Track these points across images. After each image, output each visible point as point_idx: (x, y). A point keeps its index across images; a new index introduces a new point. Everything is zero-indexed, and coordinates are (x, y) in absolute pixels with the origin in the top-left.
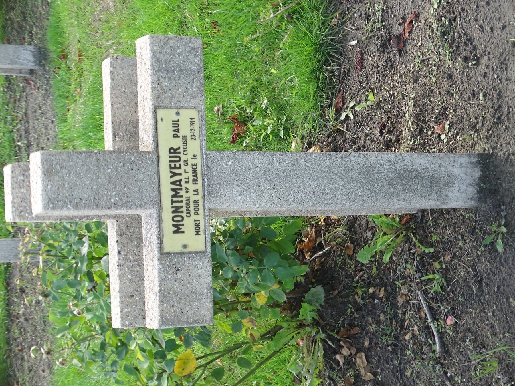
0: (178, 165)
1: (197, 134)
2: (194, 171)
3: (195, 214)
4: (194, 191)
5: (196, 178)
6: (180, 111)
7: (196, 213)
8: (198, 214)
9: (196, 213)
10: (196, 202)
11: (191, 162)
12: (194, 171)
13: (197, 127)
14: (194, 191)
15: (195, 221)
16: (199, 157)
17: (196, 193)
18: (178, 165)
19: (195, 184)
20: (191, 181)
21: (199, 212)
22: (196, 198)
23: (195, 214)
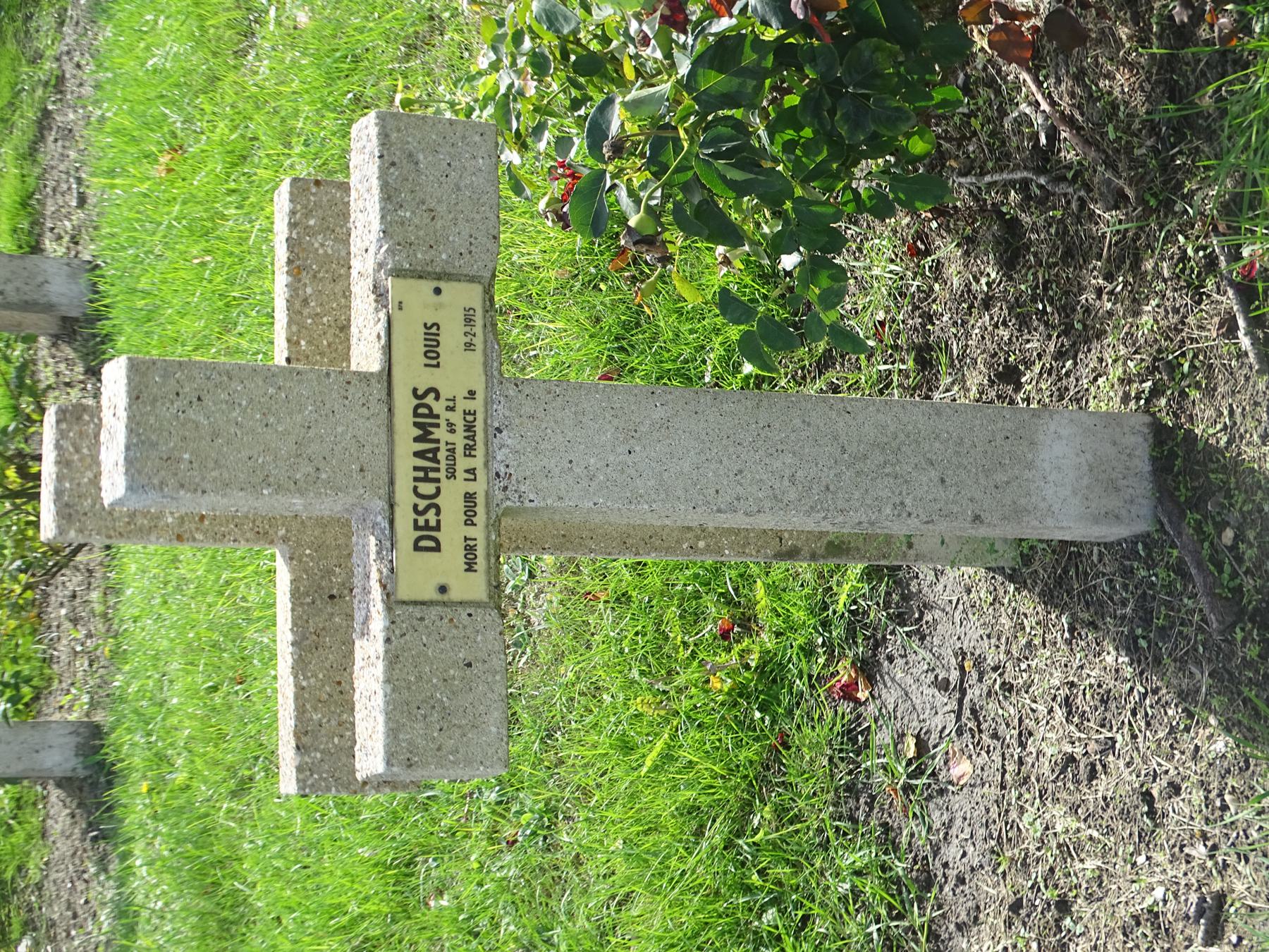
1: (478, 341)
2: (469, 428)
4: (467, 471)
5: (471, 443)
7: (469, 522)
8: (473, 524)
9: (469, 522)
11: (462, 405)
12: (469, 428)
14: (467, 471)
16: (480, 396)
19: (470, 455)
20: (460, 450)
21: (475, 520)
22: (471, 488)
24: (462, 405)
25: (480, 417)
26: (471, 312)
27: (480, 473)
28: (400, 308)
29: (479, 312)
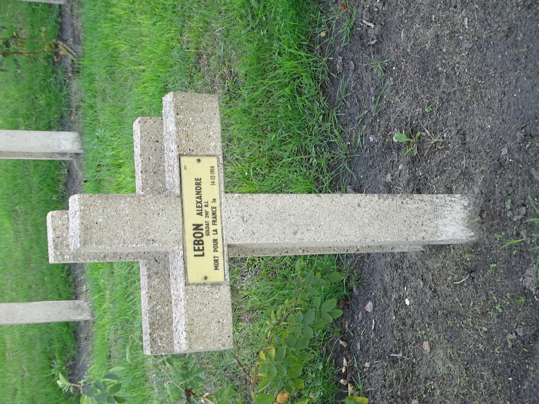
2: (214, 214)
4: (214, 231)
5: (215, 220)
6: (202, 159)
7: (215, 250)
8: (217, 251)
9: (215, 250)
10: (215, 241)
11: (211, 205)
12: (214, 214)
13: (216, 174)
14: (214, 231)
16: (218, 201)
20: (210, 223)
21: (217, 249)
22: (215, 237)
24: (211, 205)
25: (217, 209)
27: (219, 231)
28: (185, 168)
29: (216, 169)
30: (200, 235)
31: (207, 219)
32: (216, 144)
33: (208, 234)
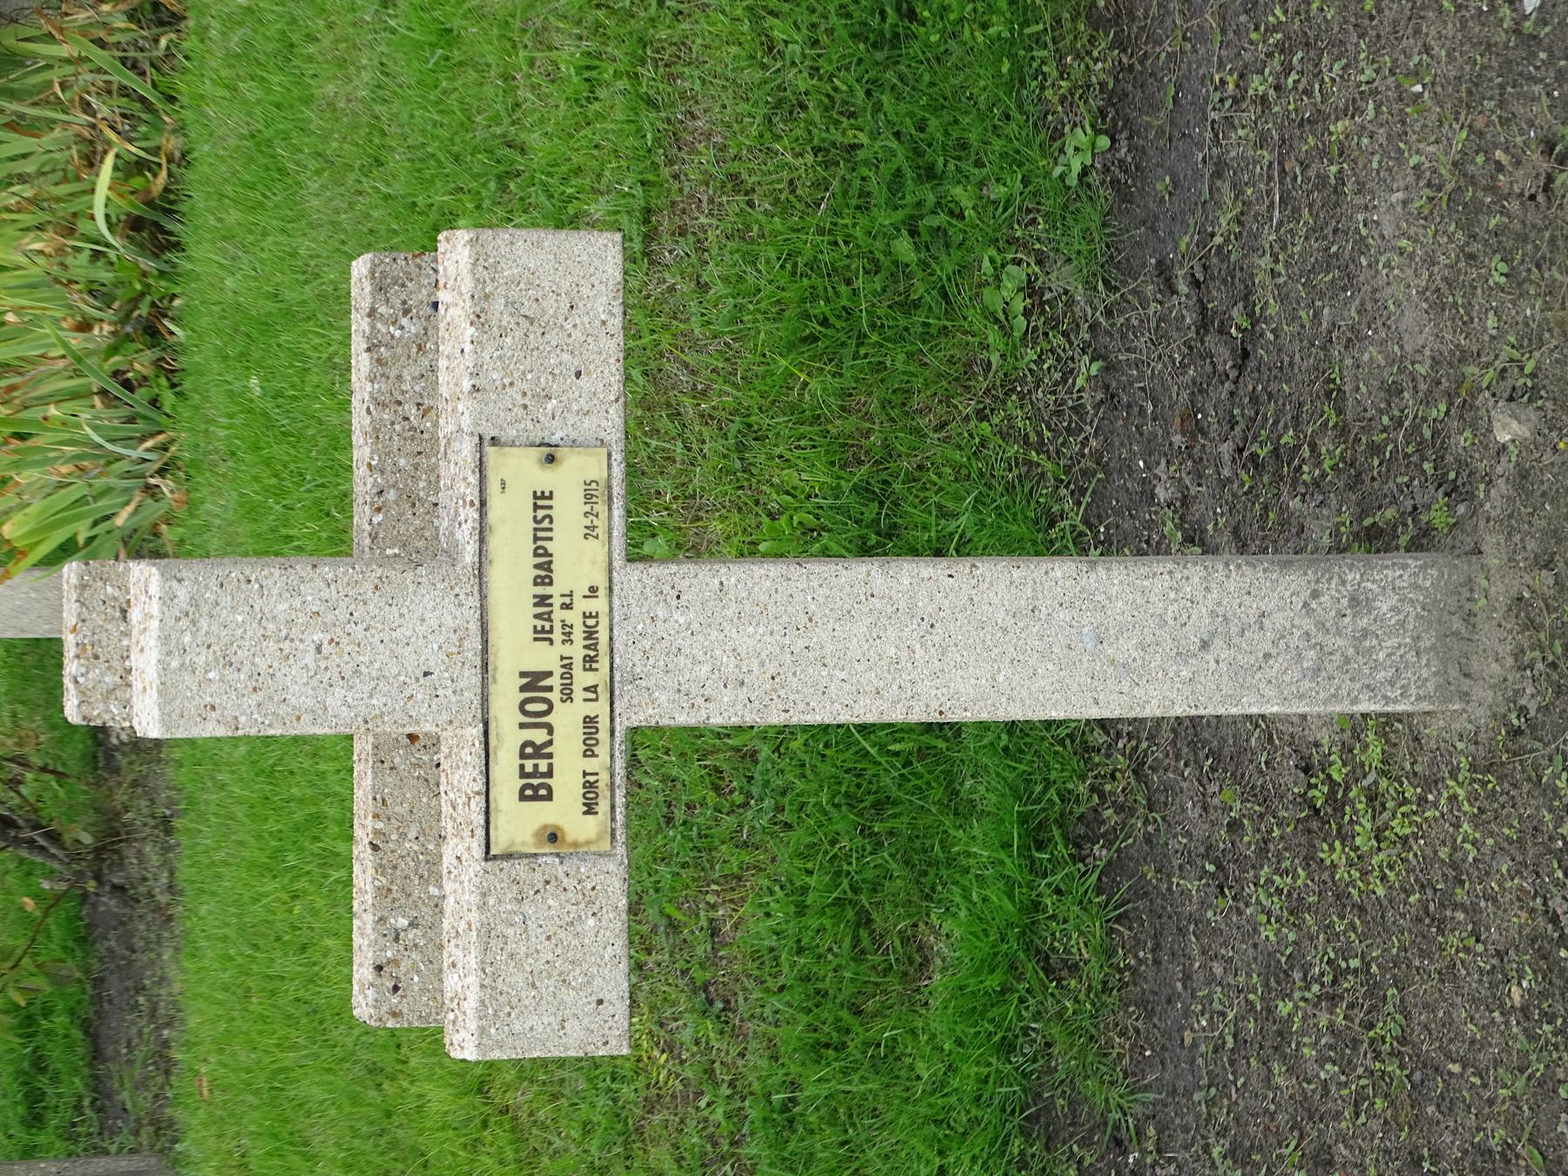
0: (543, 768)
1: (601, 524)
2: (590, 634)
3: (585, 756)
4: (586, 689)
6: (559, 452)
7: (589, 753)
8: (594, 755)
11: (581, 605)
12: (590, 634)
14: (586, 689)
15: (585, 774)
16: (602, 592)
17: (593, 696)
18: (543, 768)
19: (591, 669)
22: (590, 709)
23: (585, 756)
26: (594, 486)
30: (543, 707)
31: (567, 650)
32: (604, 416)
33: (568, 697)
